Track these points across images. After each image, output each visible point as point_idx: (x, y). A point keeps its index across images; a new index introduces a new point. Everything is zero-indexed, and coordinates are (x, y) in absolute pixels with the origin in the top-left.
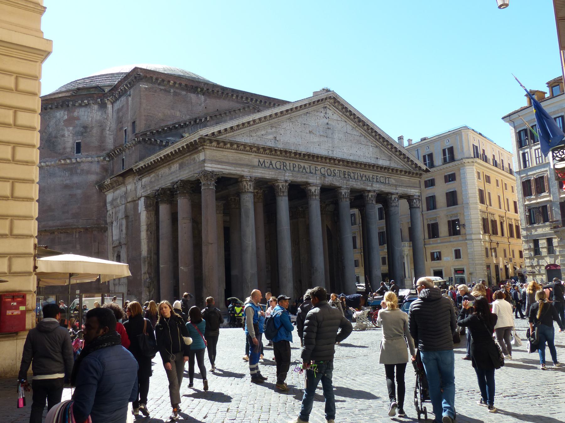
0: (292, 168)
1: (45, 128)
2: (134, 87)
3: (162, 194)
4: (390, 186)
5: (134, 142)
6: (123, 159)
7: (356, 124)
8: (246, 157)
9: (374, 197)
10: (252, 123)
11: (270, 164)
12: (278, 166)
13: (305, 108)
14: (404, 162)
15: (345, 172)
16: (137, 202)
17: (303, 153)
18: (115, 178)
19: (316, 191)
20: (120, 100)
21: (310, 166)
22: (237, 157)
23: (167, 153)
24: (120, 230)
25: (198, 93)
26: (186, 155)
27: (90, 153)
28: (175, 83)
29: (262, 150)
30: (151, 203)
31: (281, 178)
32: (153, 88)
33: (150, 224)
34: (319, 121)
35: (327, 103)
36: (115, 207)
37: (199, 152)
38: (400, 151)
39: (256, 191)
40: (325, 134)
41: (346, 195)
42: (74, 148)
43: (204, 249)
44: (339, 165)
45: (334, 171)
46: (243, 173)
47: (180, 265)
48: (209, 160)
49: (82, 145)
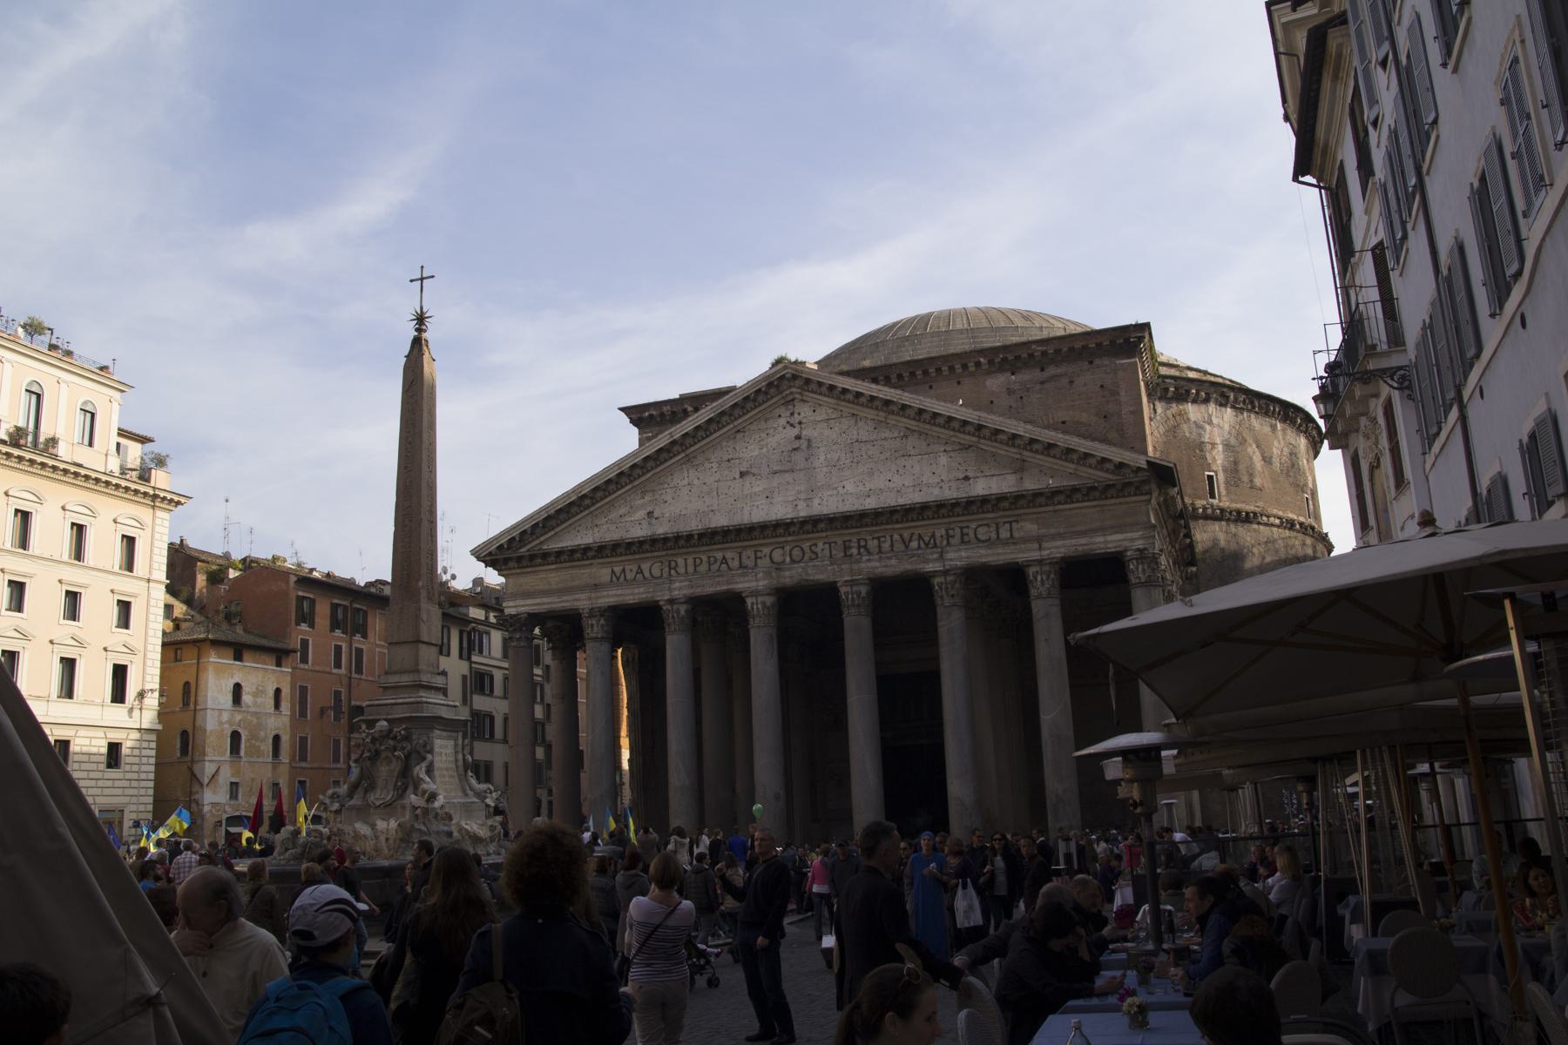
0: (691, 569)
4: (1014, 543)
9: (947, 588)
11: (637, 573)
12: (656, 572)
13: (724, 426)
15: (850, 541)
17: (695, 532)
19: (755, 607)
21: (740, 554)
30: (631, 659)
31: (662, 596)
34: (769, 440)
41: (848, 600)
44: (818, 532)
45: (813, 548)
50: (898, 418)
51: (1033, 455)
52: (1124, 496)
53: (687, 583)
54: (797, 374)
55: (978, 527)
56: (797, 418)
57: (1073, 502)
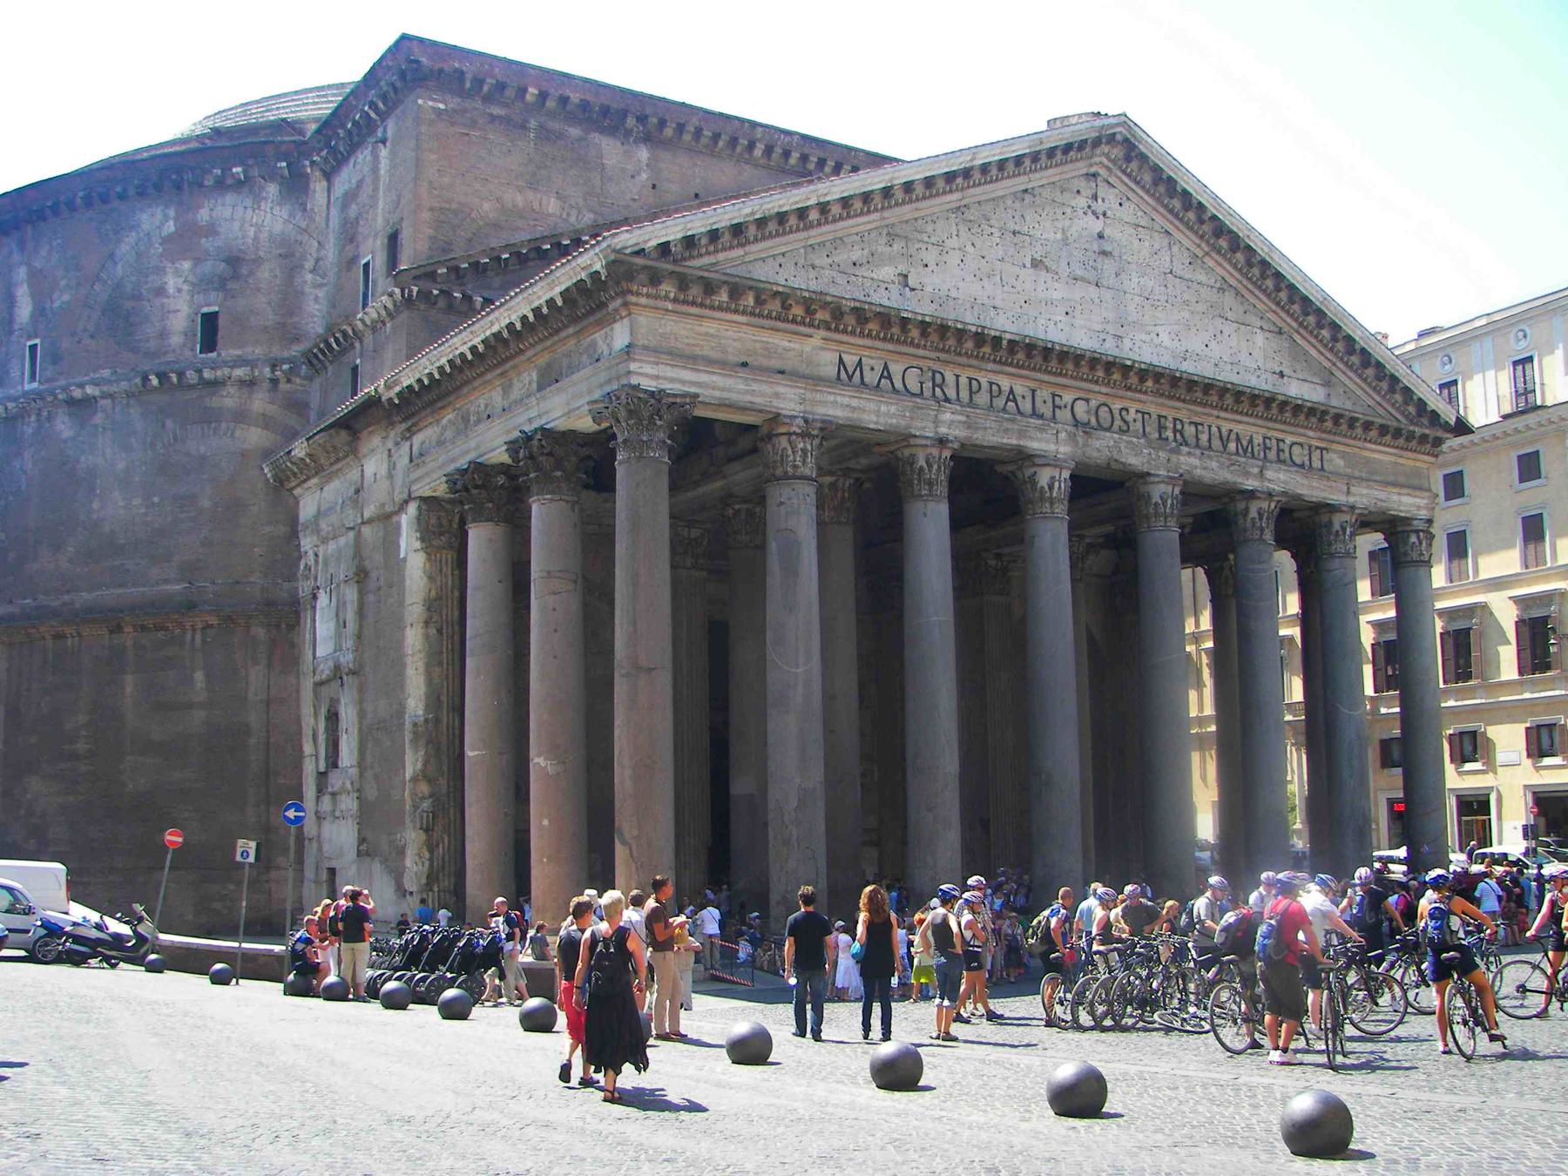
0: (964, 395)
1: (103, 266)
2: (397, 112)
3: (477, 487)
5: (390, 306)
6: (355, 369)
7: (1208, 242)
8: (792, 345)
9: (1268, 519)
10: (814, 216)
13: (1019, 175)
14: (1379, 393)
15: (1165, 417)
16: (395, 519)
17: (1008, 336)
18: (321, 435)
19: (1057, 484)
20: (352, 161)
21: (1034, 391)
22: (754, 341)
23: (495, 329)
24: (338, 621)
25: (628, 133)
26: (563, 334)
27: (249, 349)
28: (543, 96)
29: (850, 320)
31: (924, 428)
32: (465, 111)
33: (439, 598)
34: (1067, 223)
35: (1100, 160)
36: (325, 541)
37: (612, 319)
38: (1363, 351)
39: (828, 479)
40: (1091, 276)
41: (1165, 507)
42: (195, 335)
43: (620, 689)
44: (1140, 391)
45: (1124, 413)
46: (776, 403)
47: (532, 753)
48: (646, 348)
49: (222, 322)
50: (1220, 259)
51: (1344, 369)
52: (1420, 452)
53: (964, 419)
54: (1132, 140)
55: (1293, 444)
56: (1099, 207)
57: (1380, 444)
